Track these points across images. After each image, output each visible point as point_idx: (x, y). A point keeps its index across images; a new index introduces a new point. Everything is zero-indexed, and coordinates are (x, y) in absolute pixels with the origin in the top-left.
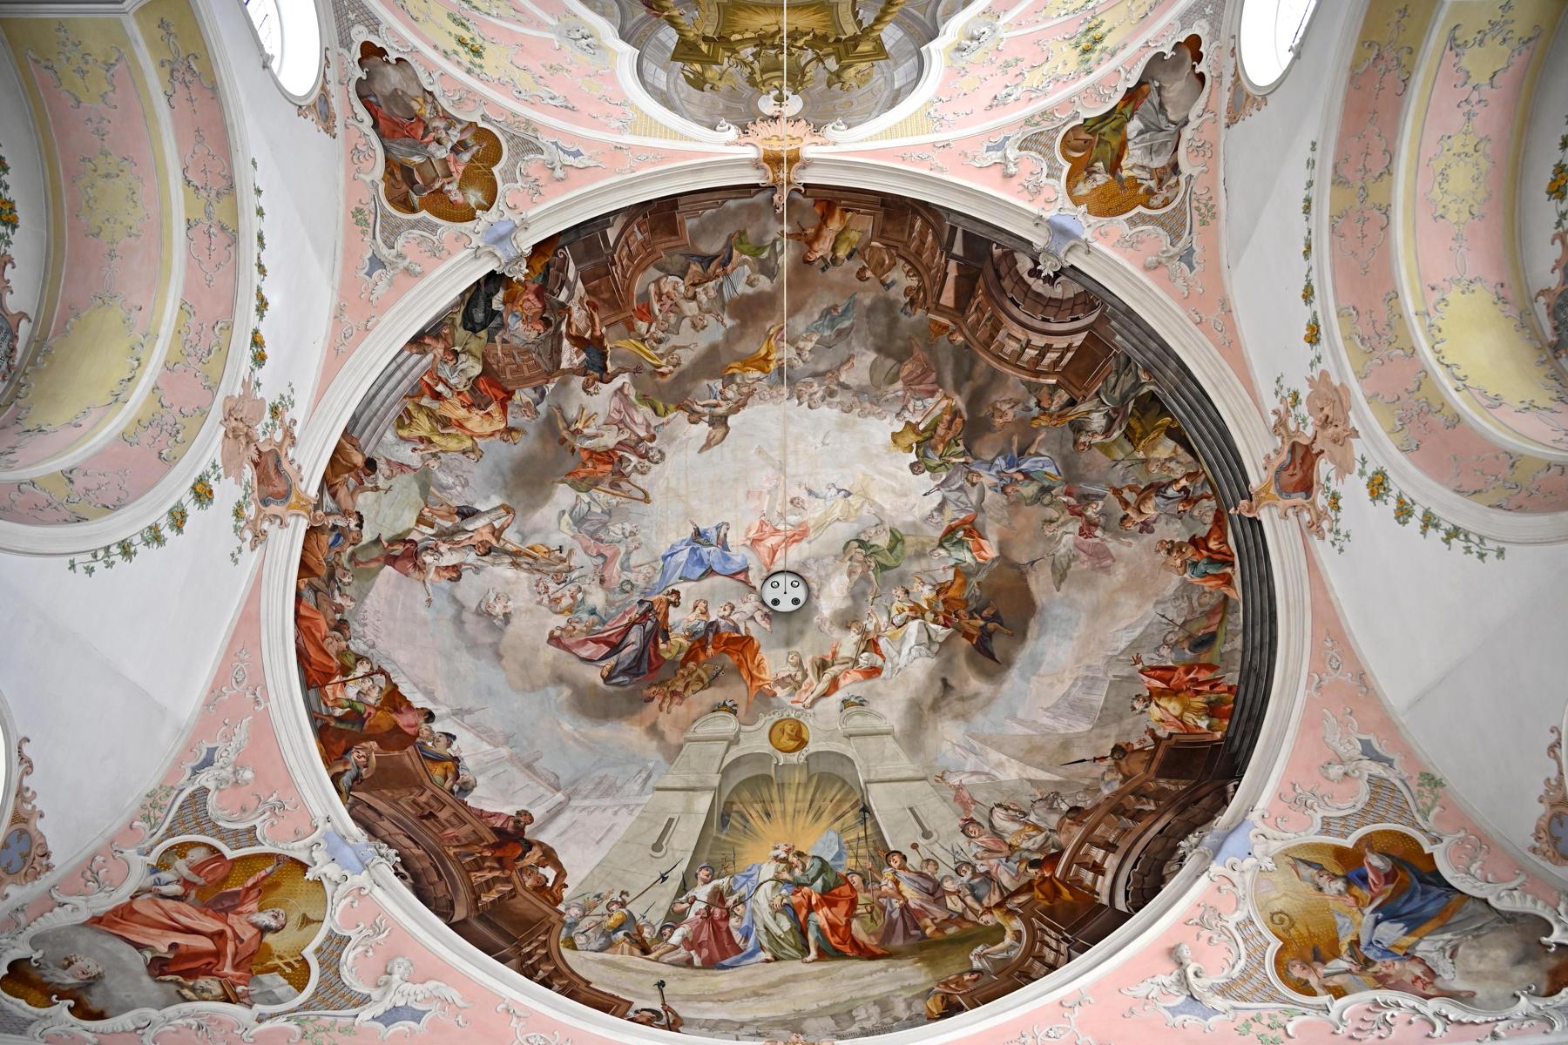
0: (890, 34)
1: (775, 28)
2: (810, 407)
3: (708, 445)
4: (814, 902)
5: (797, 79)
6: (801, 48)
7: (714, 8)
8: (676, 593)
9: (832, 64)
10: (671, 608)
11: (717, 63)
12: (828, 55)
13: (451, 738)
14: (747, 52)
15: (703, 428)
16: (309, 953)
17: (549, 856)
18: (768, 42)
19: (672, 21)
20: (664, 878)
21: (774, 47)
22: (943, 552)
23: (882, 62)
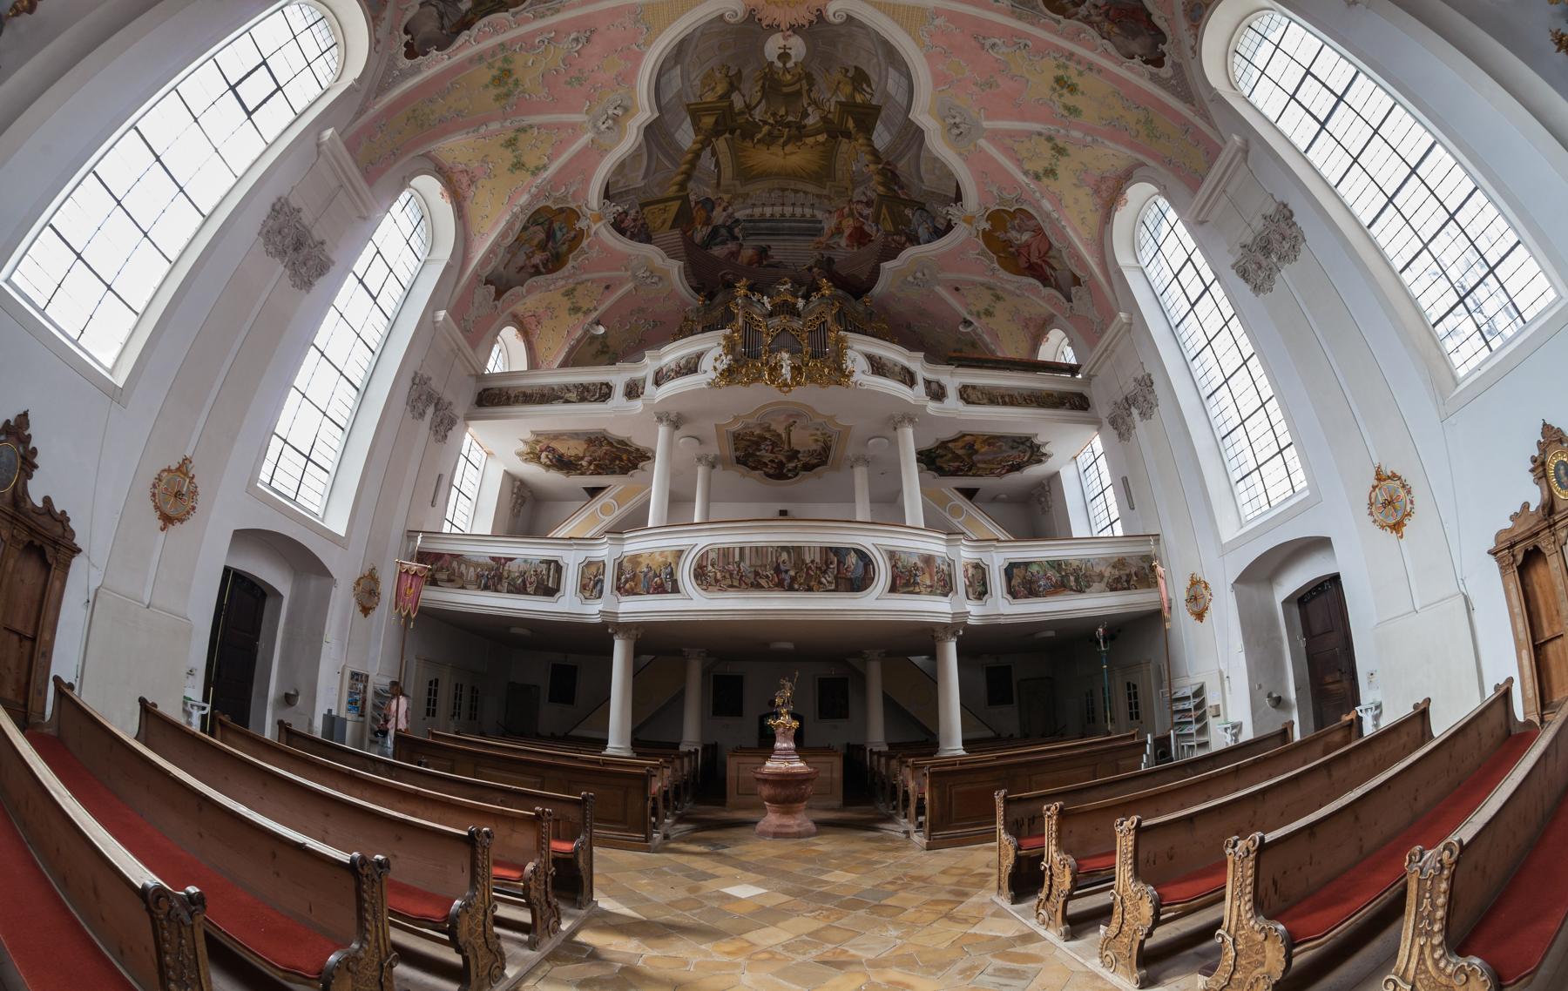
0: (686, 136)
1: (788, 148)
5: (771, 84)
6: (765, 123)
7: (839, 174)
9: (738, 101)
11: (840, 103)
12: (741, 113)
14: (812, 120)
18: (794, 131)
19: (874, 152)
21: (789, 125)
23: (693, 100)
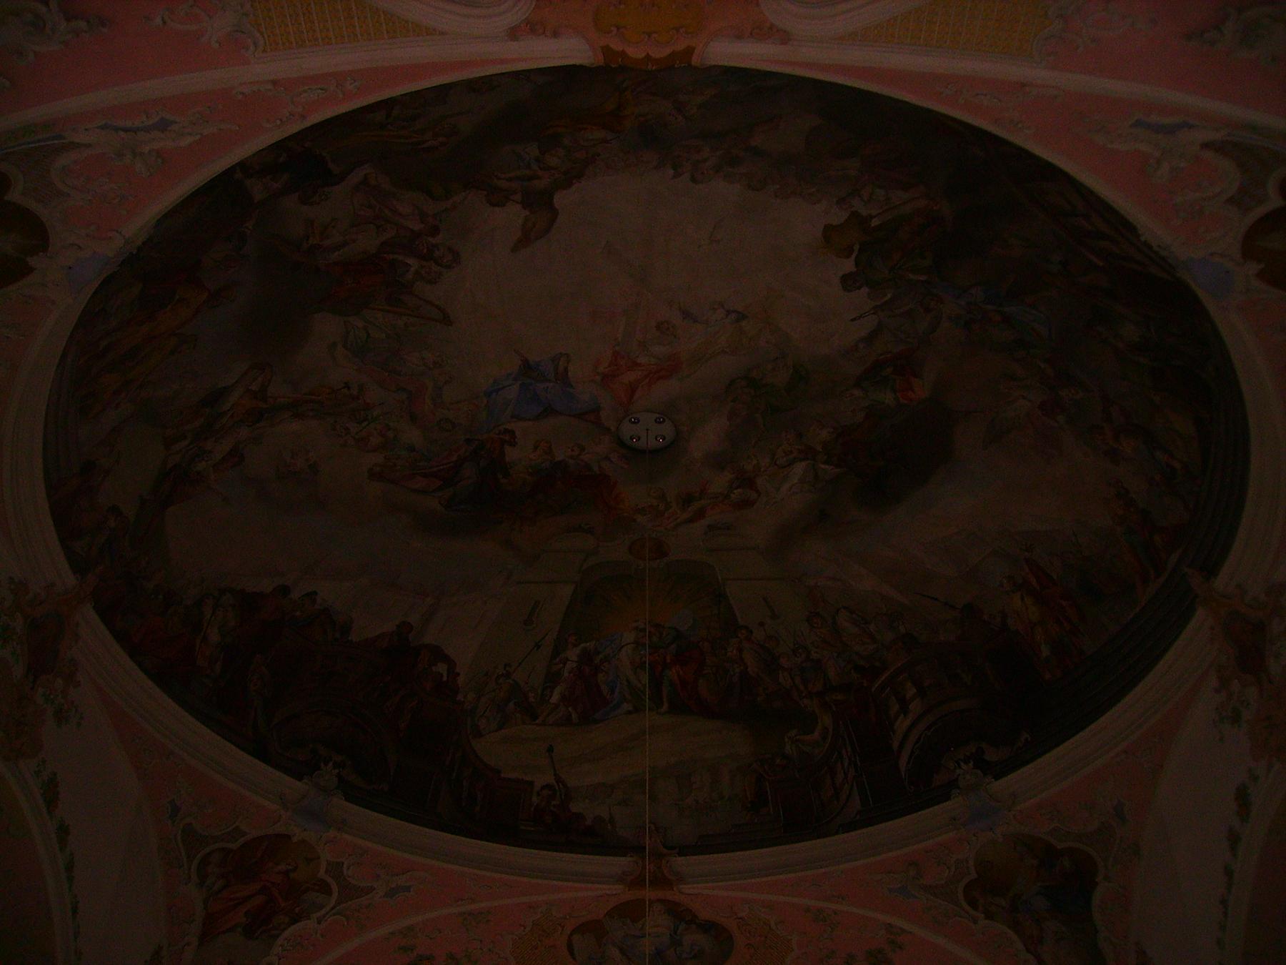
2: (694, 180)
3: (526, 239)
4: (668, 661)
8: (512, 433)
10: (507, 449)
13: (312, 595)
15: (512, 216)
16: (322, 873)
17: (438, 654)
20: (538, 646)
22: (857, 392)
